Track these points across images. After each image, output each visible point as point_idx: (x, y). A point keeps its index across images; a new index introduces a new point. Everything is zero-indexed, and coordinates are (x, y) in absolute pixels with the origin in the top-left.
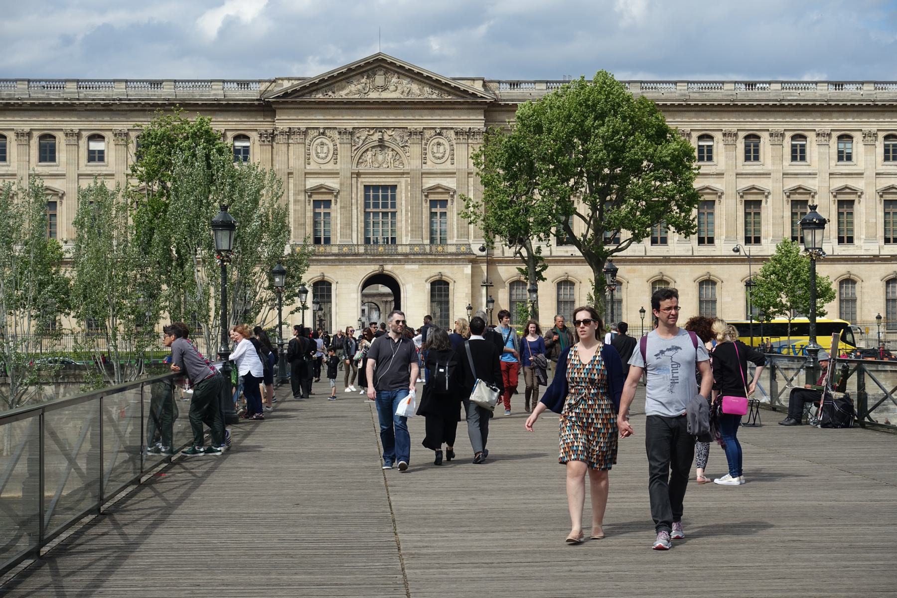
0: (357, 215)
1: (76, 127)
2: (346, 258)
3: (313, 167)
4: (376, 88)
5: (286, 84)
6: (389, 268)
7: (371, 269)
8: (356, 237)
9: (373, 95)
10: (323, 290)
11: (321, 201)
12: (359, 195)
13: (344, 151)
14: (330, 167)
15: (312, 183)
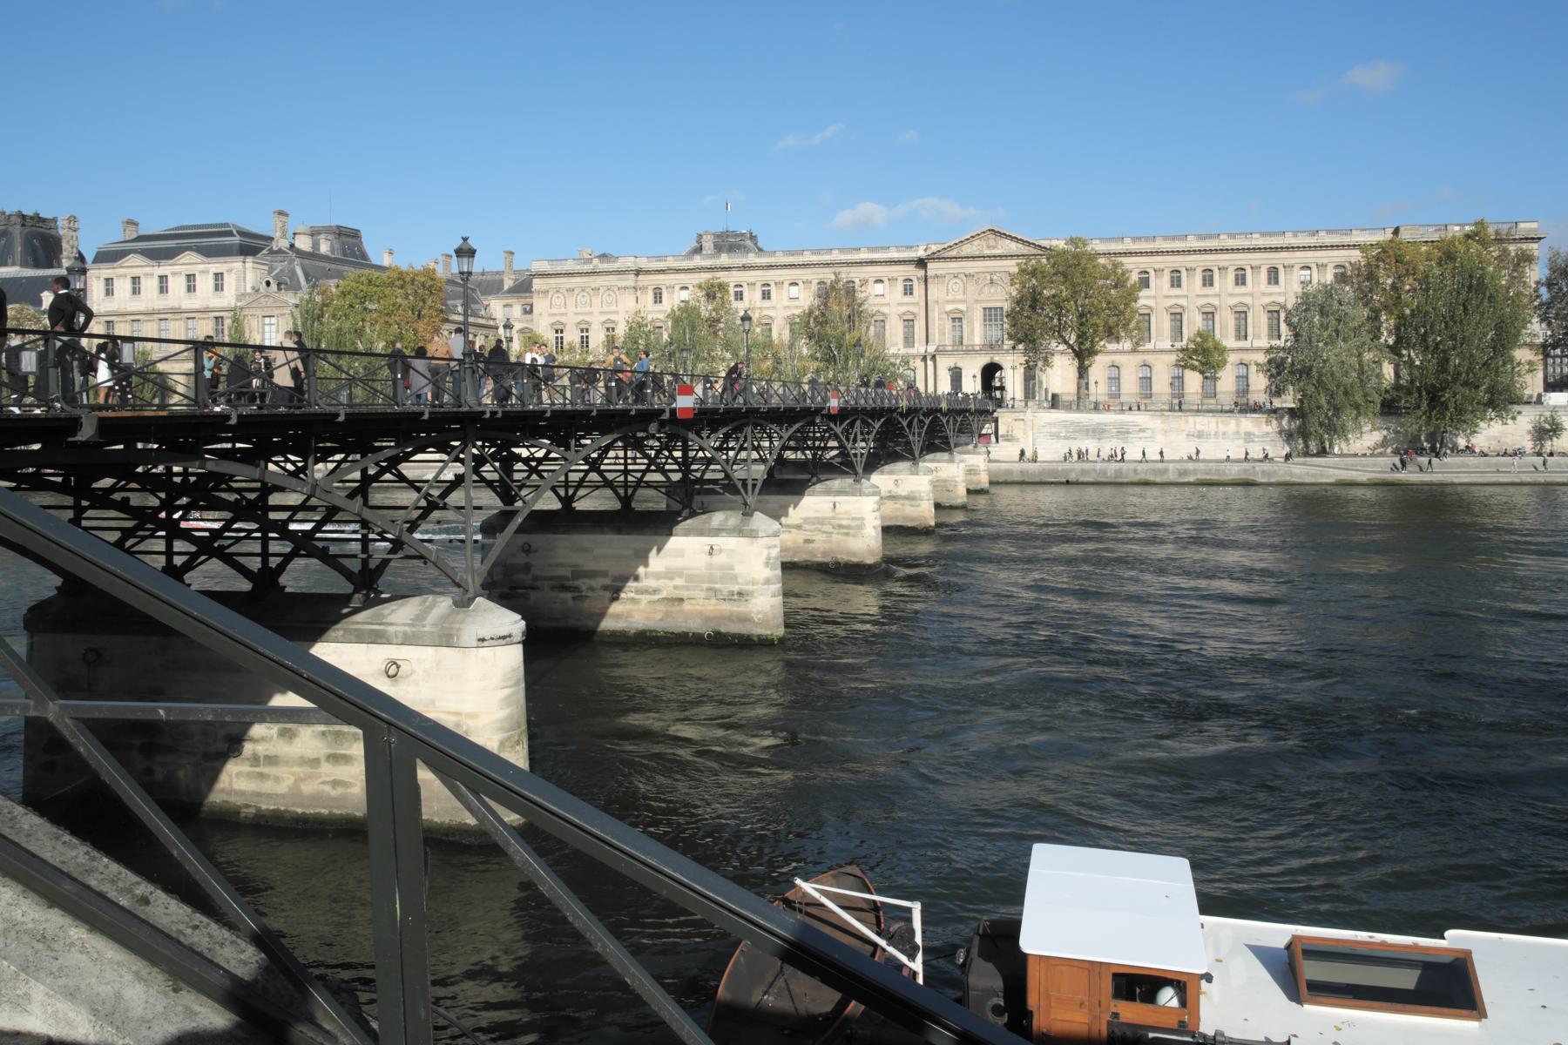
0: (978, 326)
1: (809, 278)
2: (970, 351)
3: (950, 297)
4: (989, 247)
5: (934, 248)
6: (997, 359)
7: (984, 360)
8: (978, 340)
9: (987, 252)
10: (956, 376)
11: (957, 320)
12: (978, 314)
13: (971, 287)
14: (961, 297)
15: (949, 307)
